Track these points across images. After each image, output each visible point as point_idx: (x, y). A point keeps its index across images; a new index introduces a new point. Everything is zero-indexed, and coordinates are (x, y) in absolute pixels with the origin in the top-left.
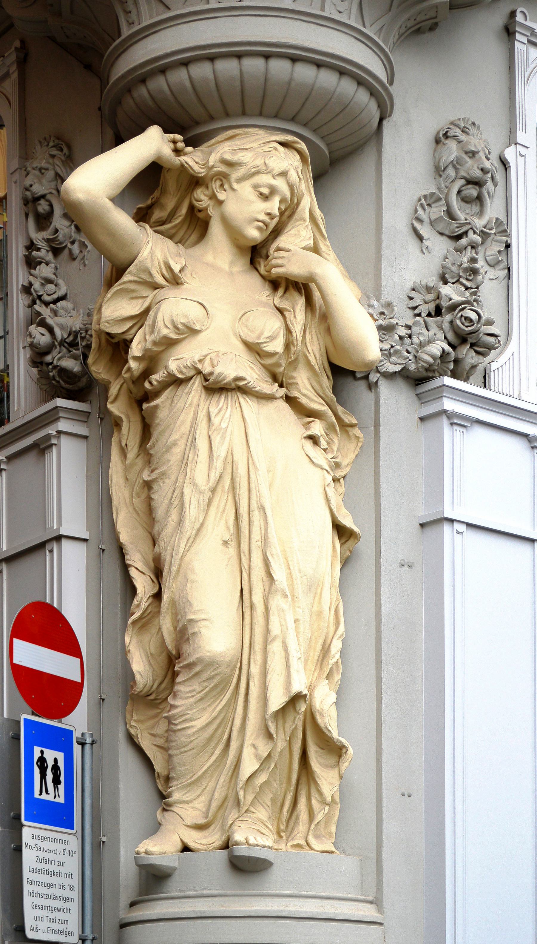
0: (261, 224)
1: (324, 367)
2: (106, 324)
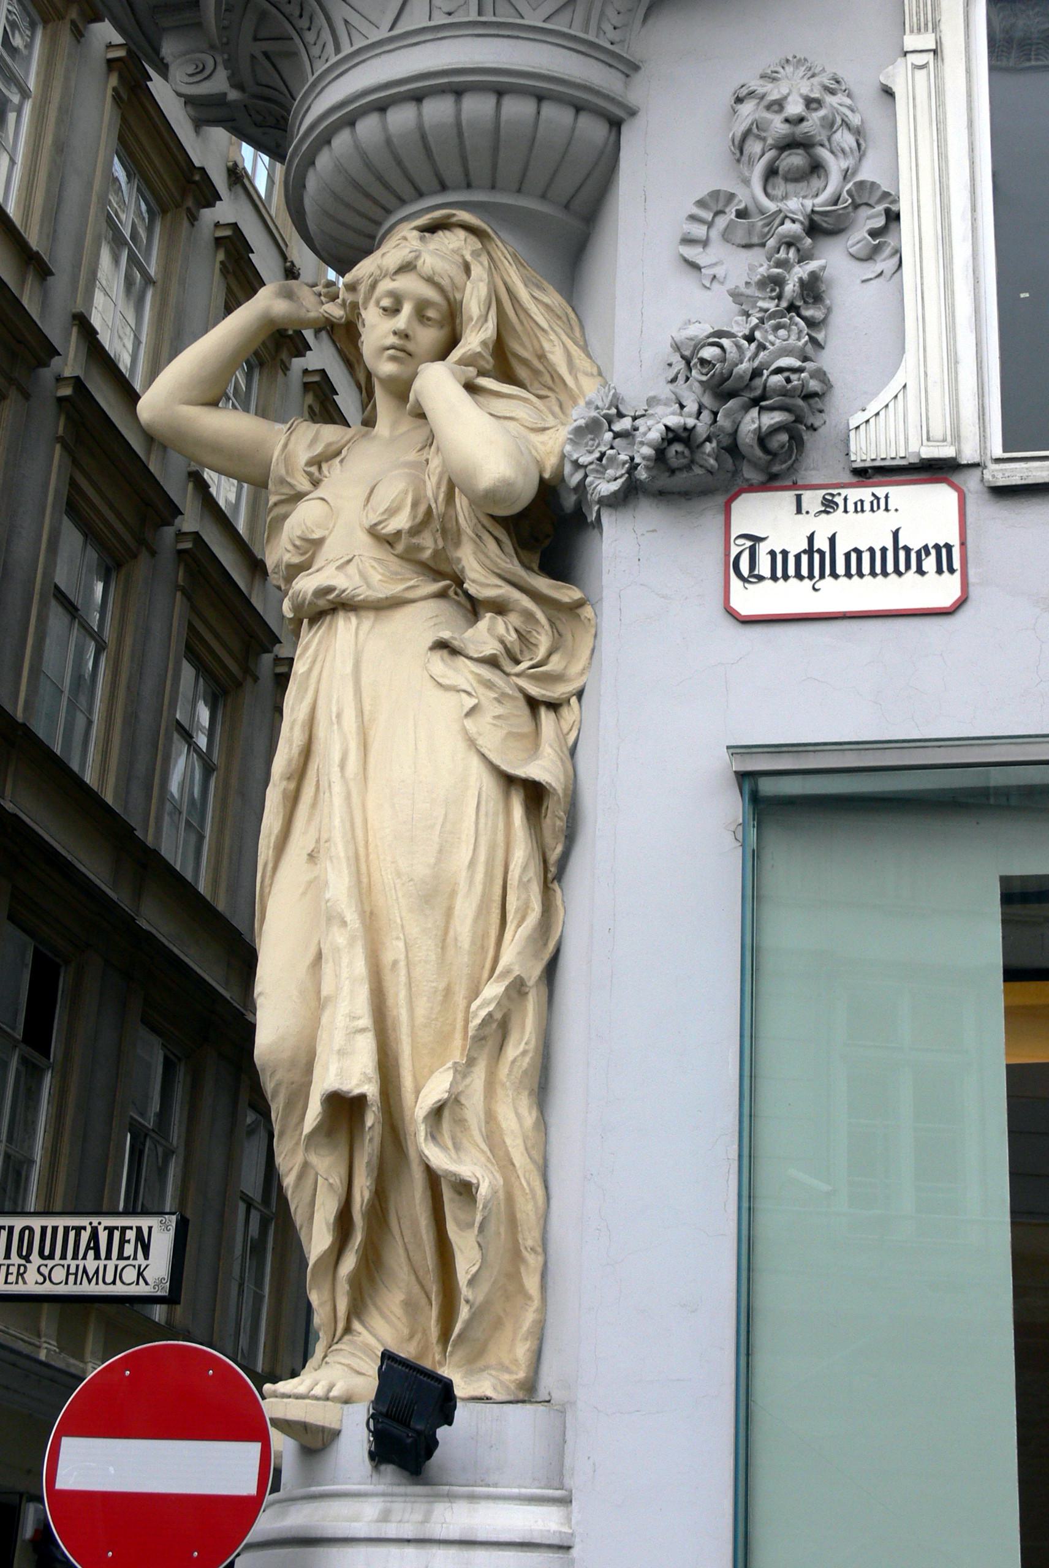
1: (484, 527)
2: (276, 576)
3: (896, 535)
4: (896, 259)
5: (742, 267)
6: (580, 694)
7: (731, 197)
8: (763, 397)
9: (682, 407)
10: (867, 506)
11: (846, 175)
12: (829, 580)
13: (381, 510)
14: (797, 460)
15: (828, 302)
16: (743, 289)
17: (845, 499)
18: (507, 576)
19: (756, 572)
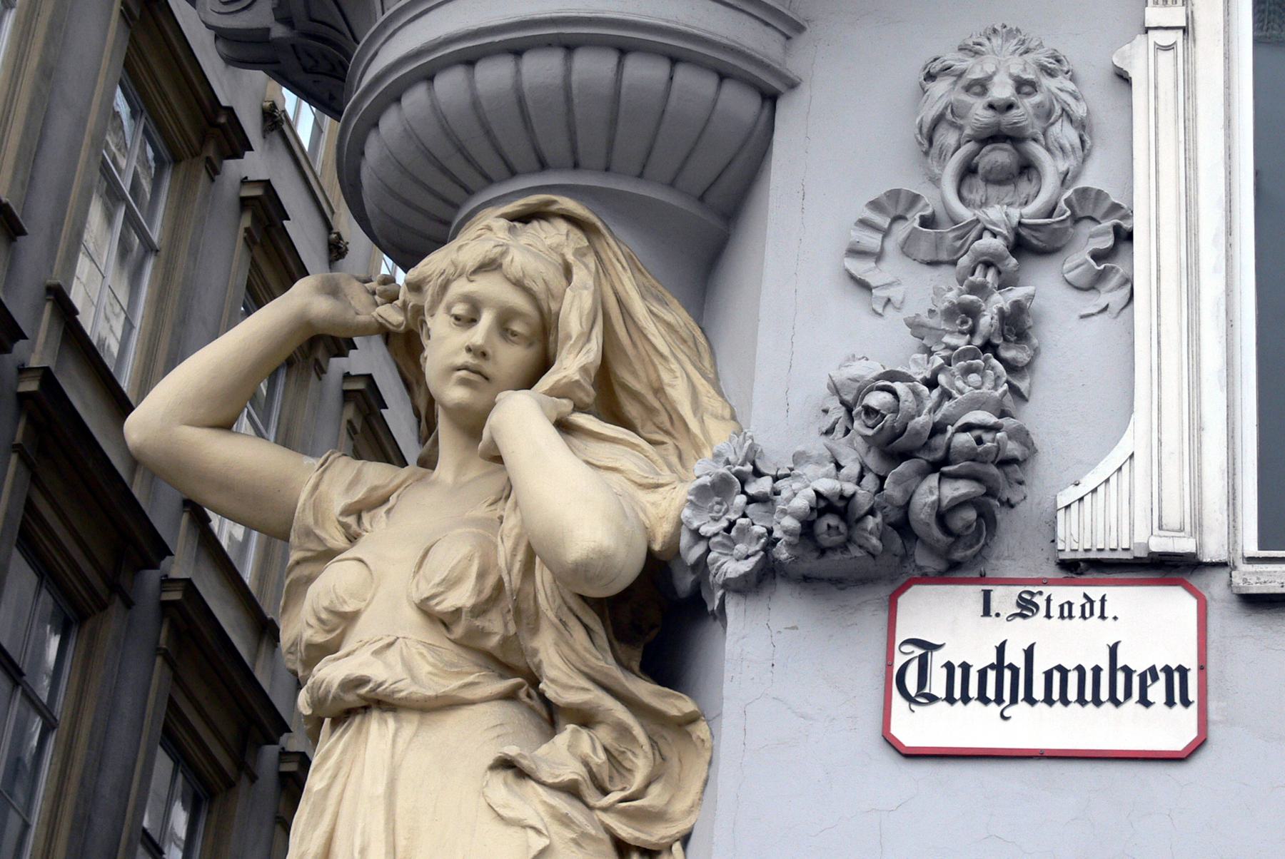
0: (463, 373)
1: (570, 609)
2: (290, 656)
3: (1113, 650)
4: (1126, 290)
5: (924, 290)
6: (685, 839)
7: (915, 199)
8: (946, 461)
9: (839, 467)
10: (1077, 611)
11: (1065, 180)
12: (1022, 706)
13: (437, 579)
14: (986, 544)
15: (1035, 341)
16: (925, 319)
17: (1049, 600)
18: (598, 677)
19: (927, 691)
